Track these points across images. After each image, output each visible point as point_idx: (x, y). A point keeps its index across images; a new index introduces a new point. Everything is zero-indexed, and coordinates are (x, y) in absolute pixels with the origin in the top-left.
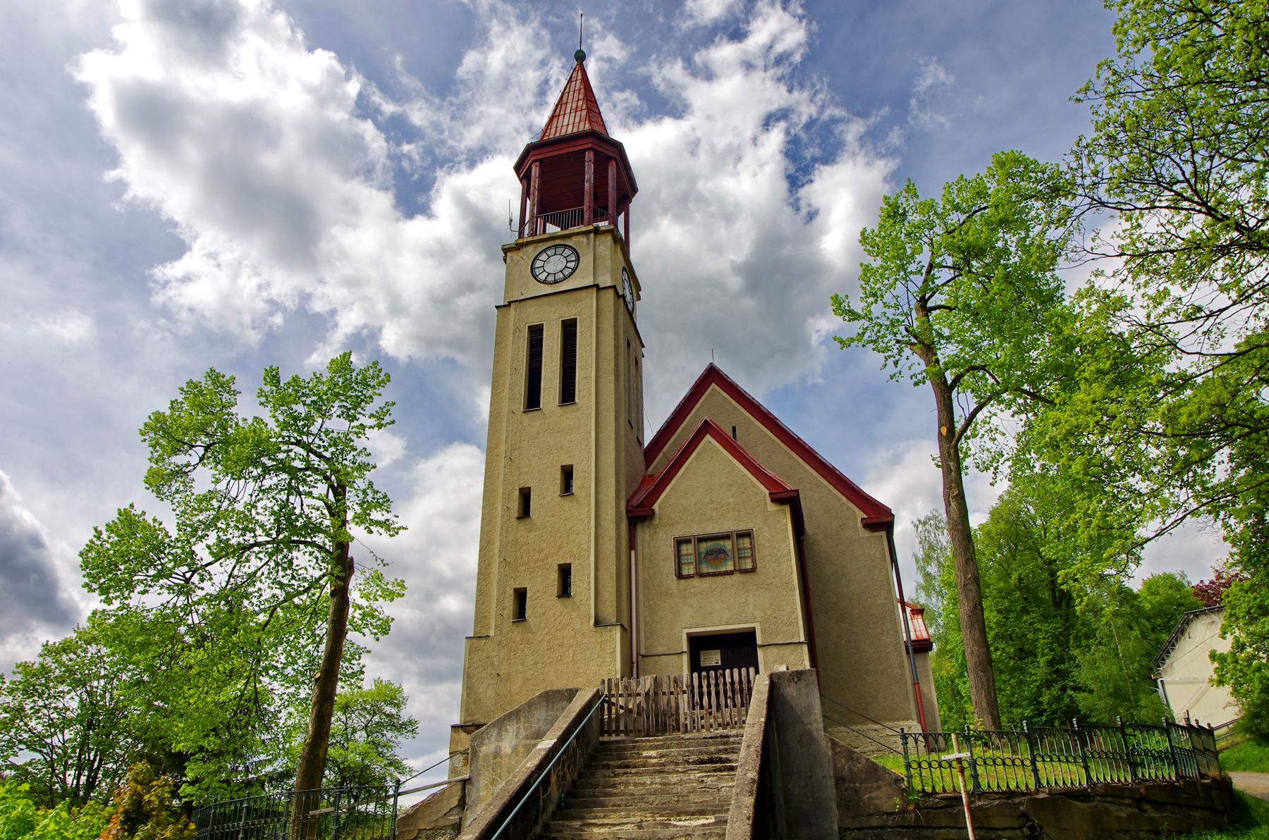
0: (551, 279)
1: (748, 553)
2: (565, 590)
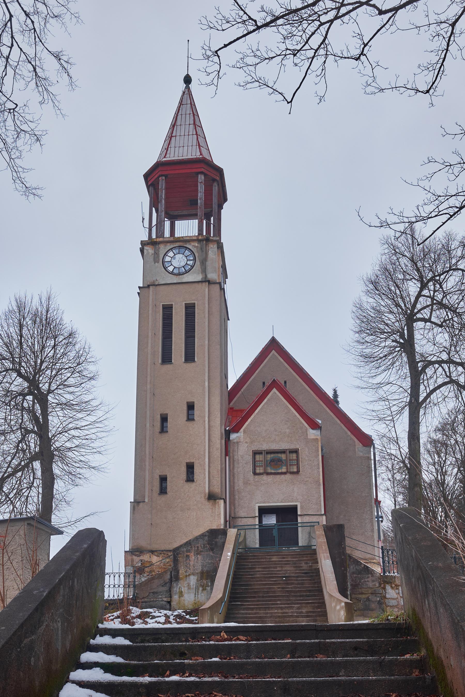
0: (176, 271)
2: (190, 477)
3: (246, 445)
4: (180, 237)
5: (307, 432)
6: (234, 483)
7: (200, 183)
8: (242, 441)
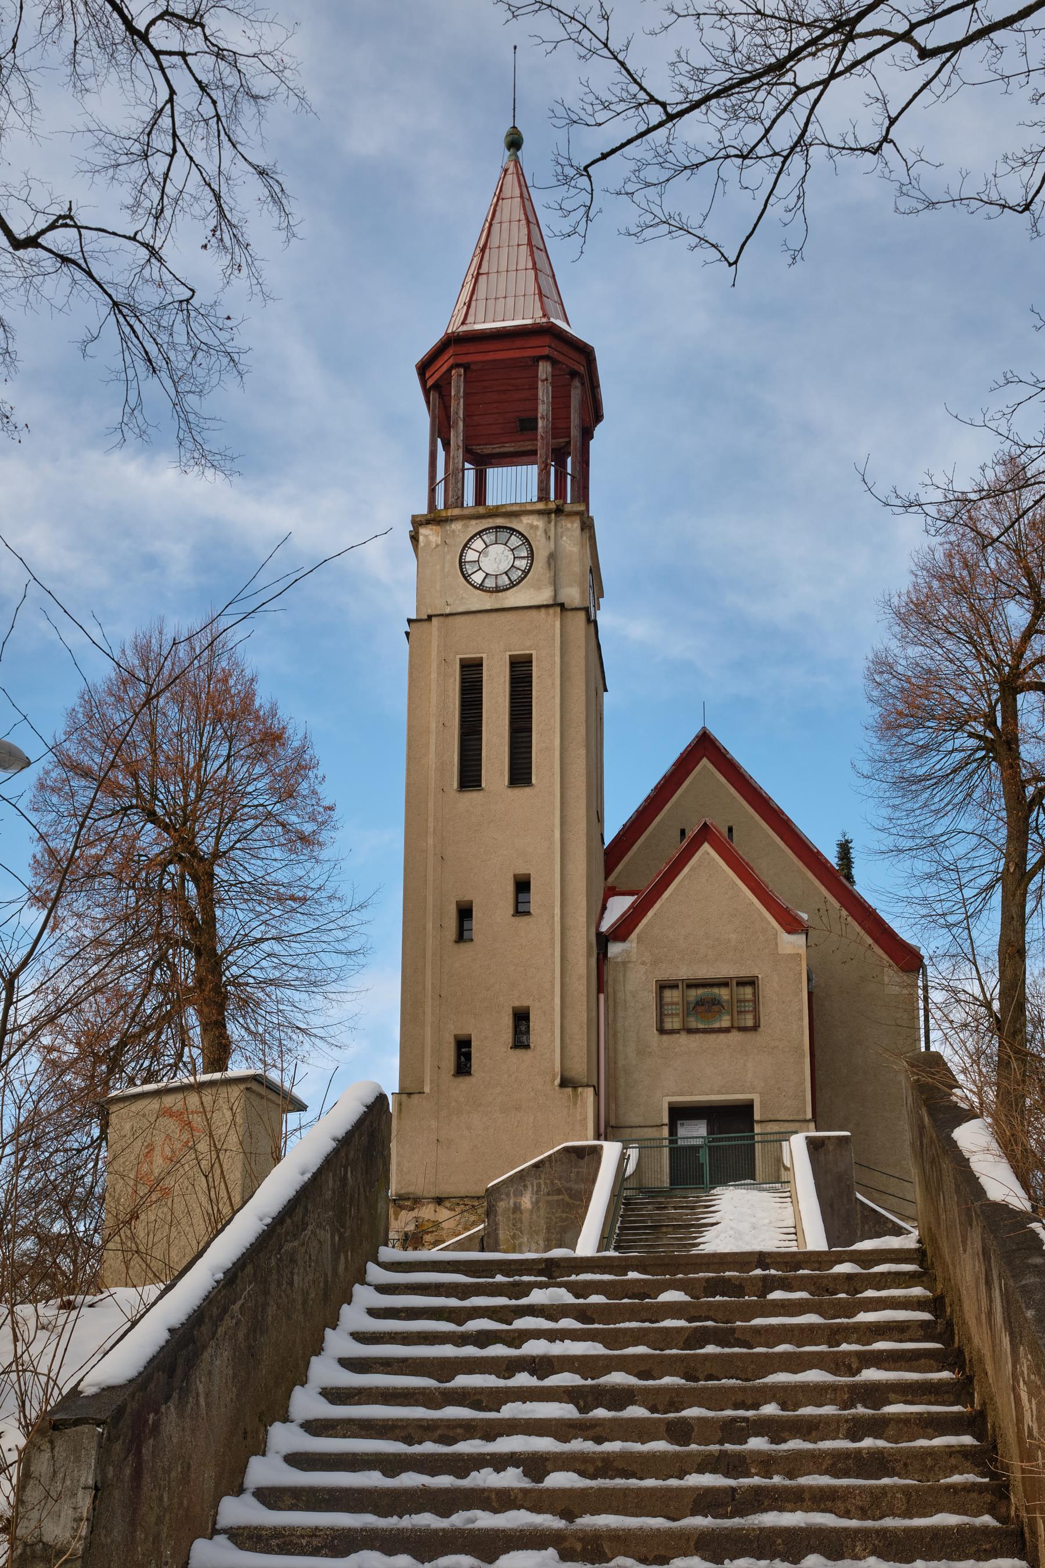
0: (490, 583)
1: (749, 1006)
2: (521, 1039)
3: (643, 969)
4: (497, 507)
5: (776, 939)
6: (616, 1050)
7: (543, 381)
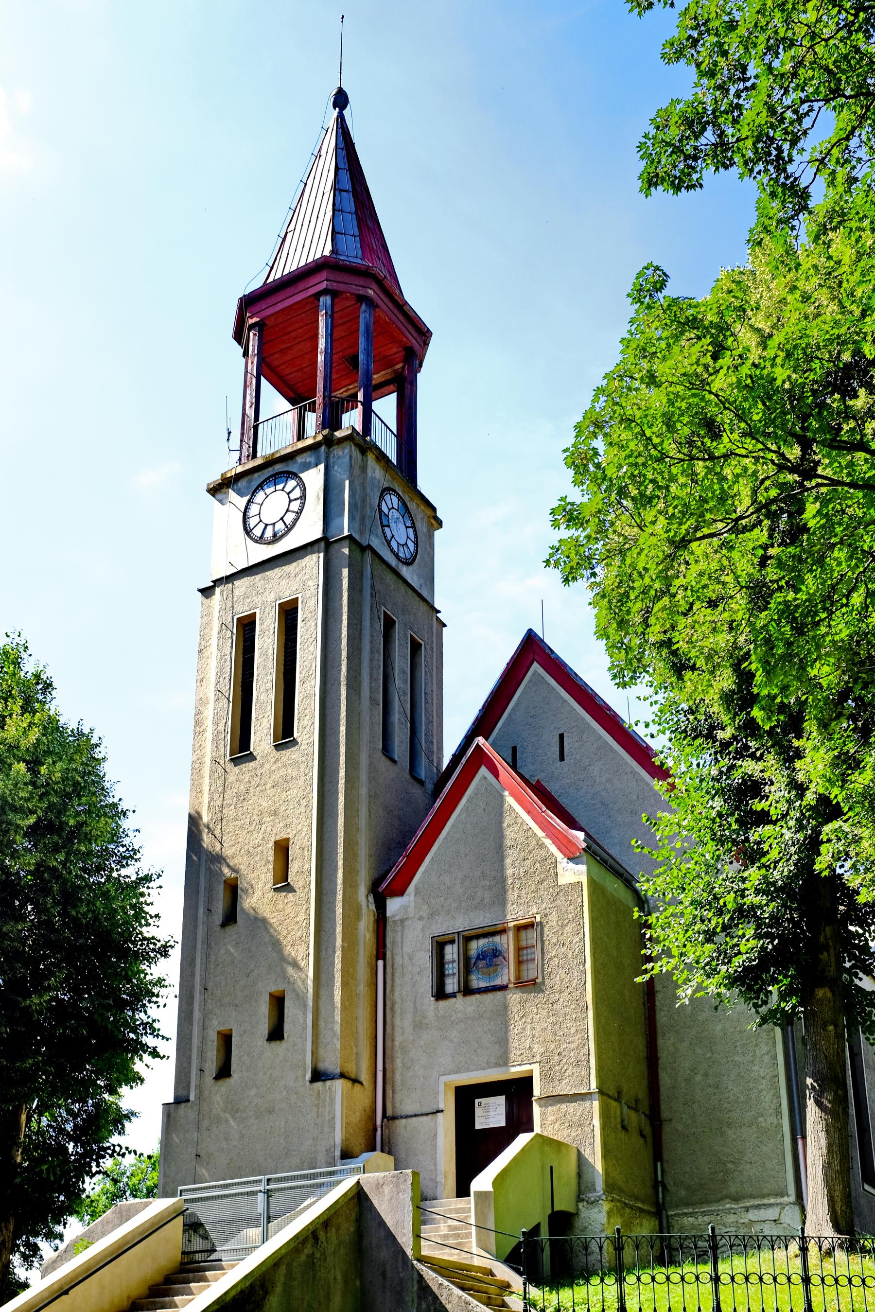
3: (419, 925)
8: (412, 915)
